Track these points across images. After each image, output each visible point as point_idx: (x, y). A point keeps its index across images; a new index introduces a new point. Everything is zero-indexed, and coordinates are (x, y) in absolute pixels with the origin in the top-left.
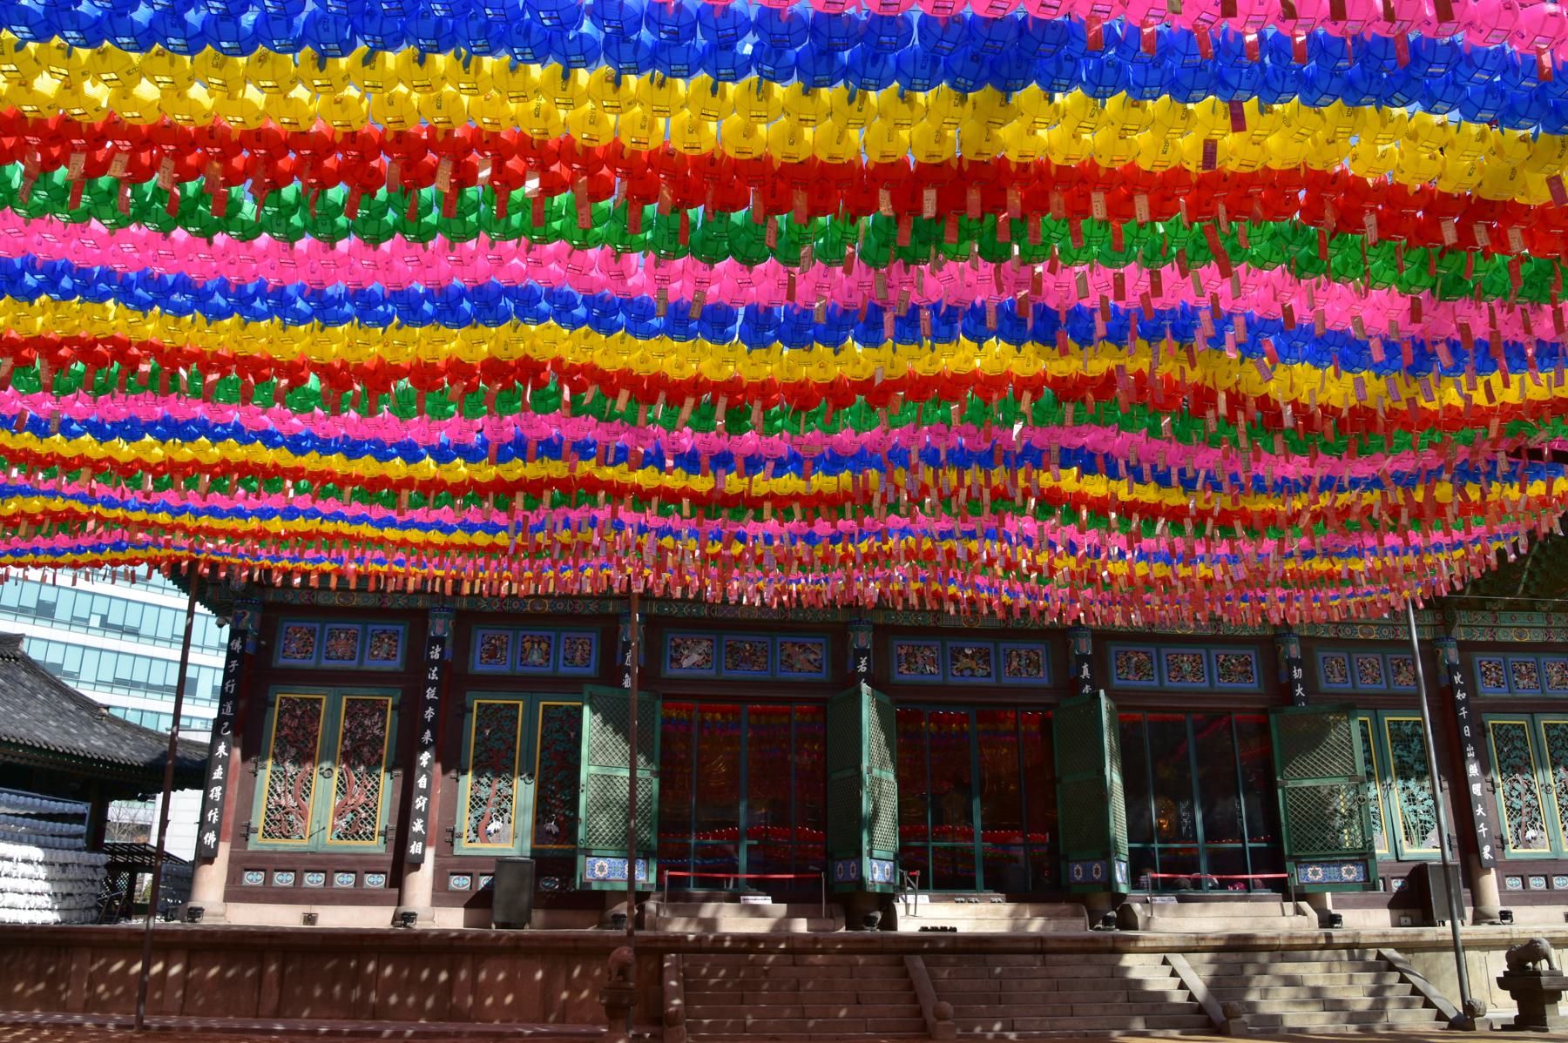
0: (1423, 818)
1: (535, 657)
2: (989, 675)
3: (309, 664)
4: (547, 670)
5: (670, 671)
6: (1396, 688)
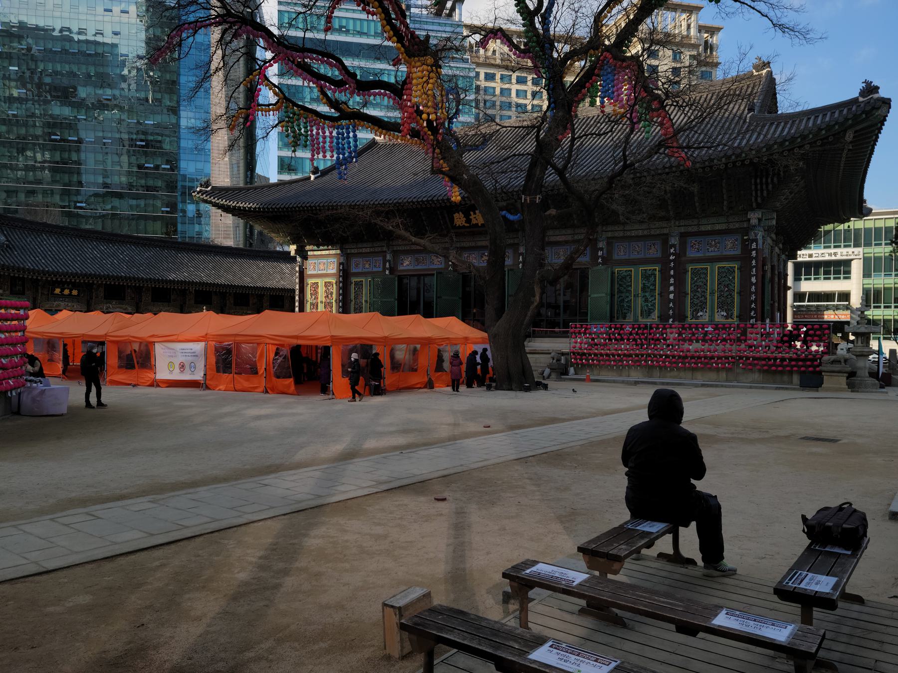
1: (367, 266)
3: (315, 272)
4: (370, 270)
5: (401, 268)
6: (648, 256)
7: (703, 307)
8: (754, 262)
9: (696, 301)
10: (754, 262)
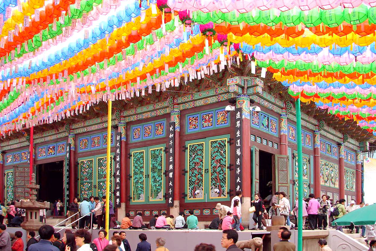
0: (158, 187)
2: (54, 154)
8: (238, 133)
9: (194, 179)
10: (238, 133)
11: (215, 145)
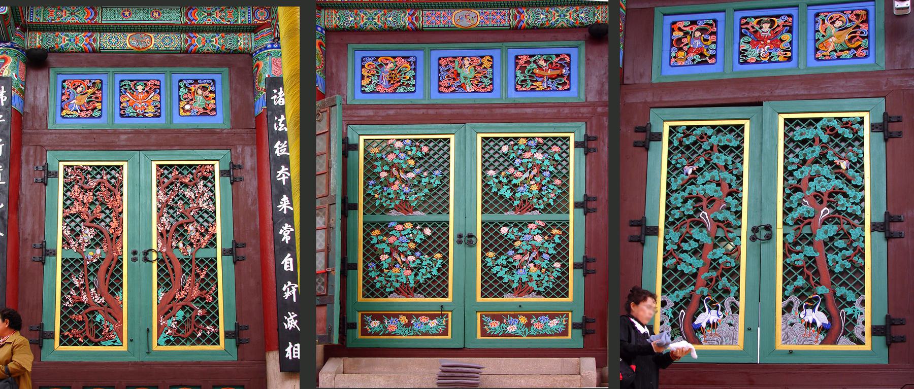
7: (719, 285)
9: (690, 264)
11: (810, 133)
